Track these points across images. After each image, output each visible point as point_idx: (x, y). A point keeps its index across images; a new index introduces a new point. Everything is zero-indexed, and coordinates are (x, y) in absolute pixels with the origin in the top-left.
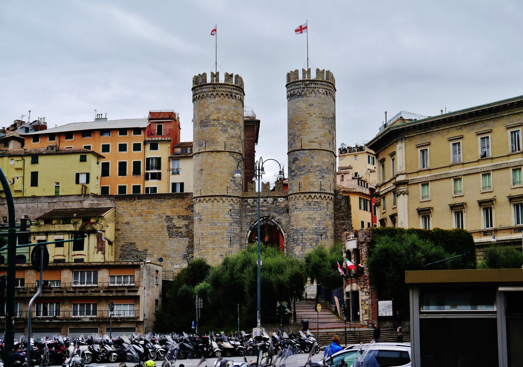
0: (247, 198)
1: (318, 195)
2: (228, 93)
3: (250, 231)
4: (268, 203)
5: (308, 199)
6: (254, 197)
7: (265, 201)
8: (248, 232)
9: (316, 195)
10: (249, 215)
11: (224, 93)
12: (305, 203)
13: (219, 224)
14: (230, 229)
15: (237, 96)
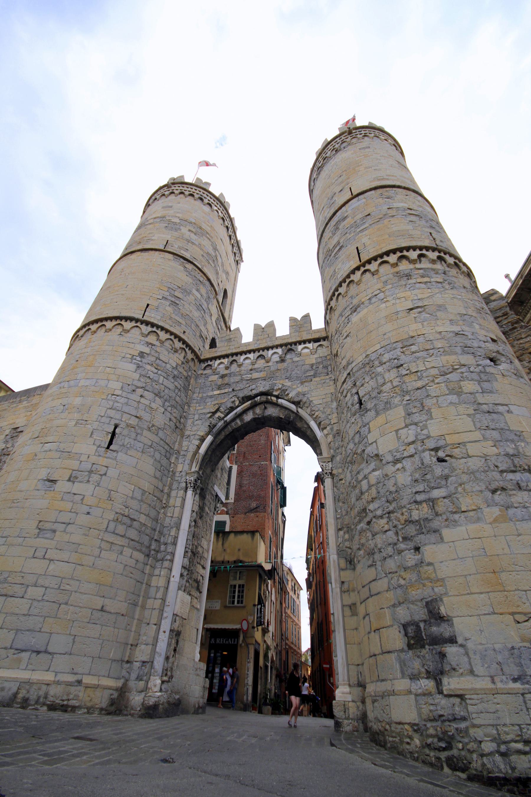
0: (211, 359)
1: (433, 255)
2: (195, 194)
3: (209, 439)
4: (268, 362)
5: (395, 265)
6: (232, 355)
7: (261, 356)
8: (202, 440)
9: (424, 252)
10: (211, 397)
11: (187, 193)
12: (384, 279)
13: (88, 383)
14: (123, 400)
15: (215, 208)
